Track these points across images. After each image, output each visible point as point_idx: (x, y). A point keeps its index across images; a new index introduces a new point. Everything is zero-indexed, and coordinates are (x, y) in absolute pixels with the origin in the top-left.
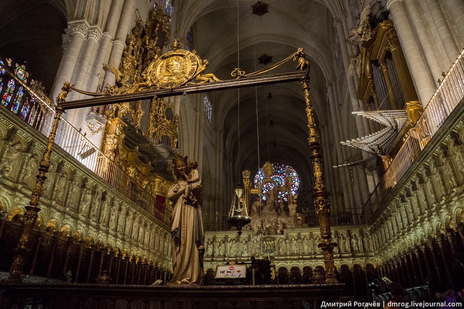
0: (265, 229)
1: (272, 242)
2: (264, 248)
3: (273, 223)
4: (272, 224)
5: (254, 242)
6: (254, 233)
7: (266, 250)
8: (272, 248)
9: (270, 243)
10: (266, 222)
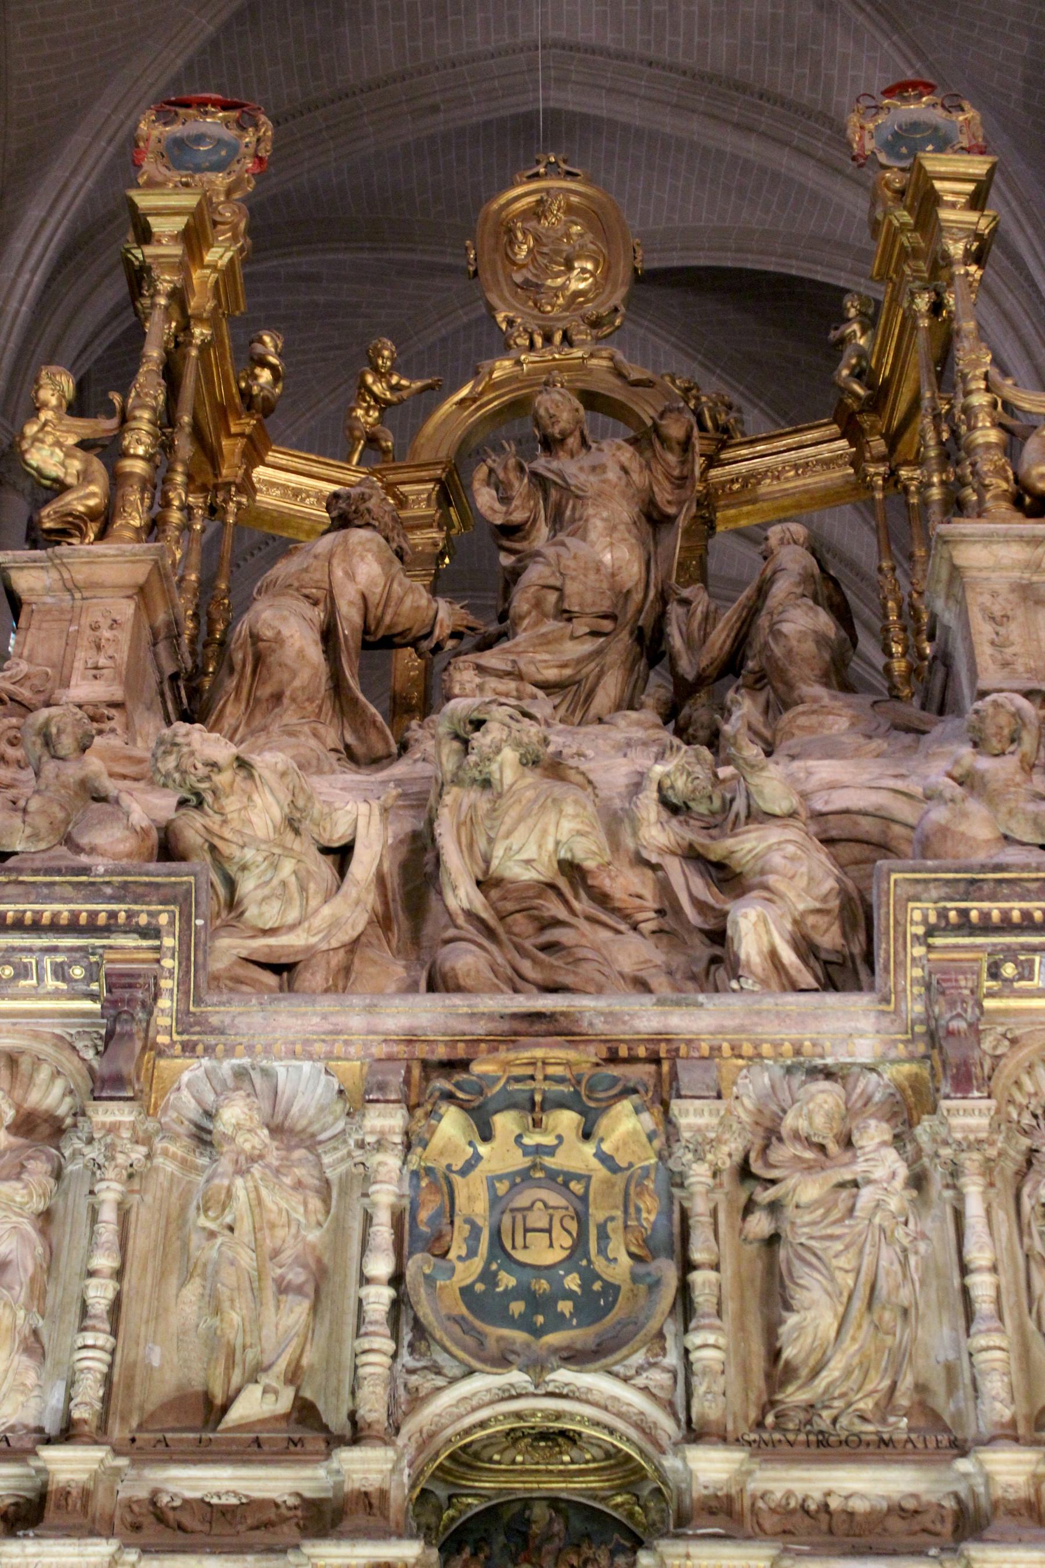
0: (461, 893)
1: (626, 1125)
2: (437, 1246)
3: (649, 807)
4: (615, 822)
5: (203, 1137)
6: (229, 948)
7: (482, 1302)
8: (617, 1265)
9: (579, 1157)
10: (506, 766)
